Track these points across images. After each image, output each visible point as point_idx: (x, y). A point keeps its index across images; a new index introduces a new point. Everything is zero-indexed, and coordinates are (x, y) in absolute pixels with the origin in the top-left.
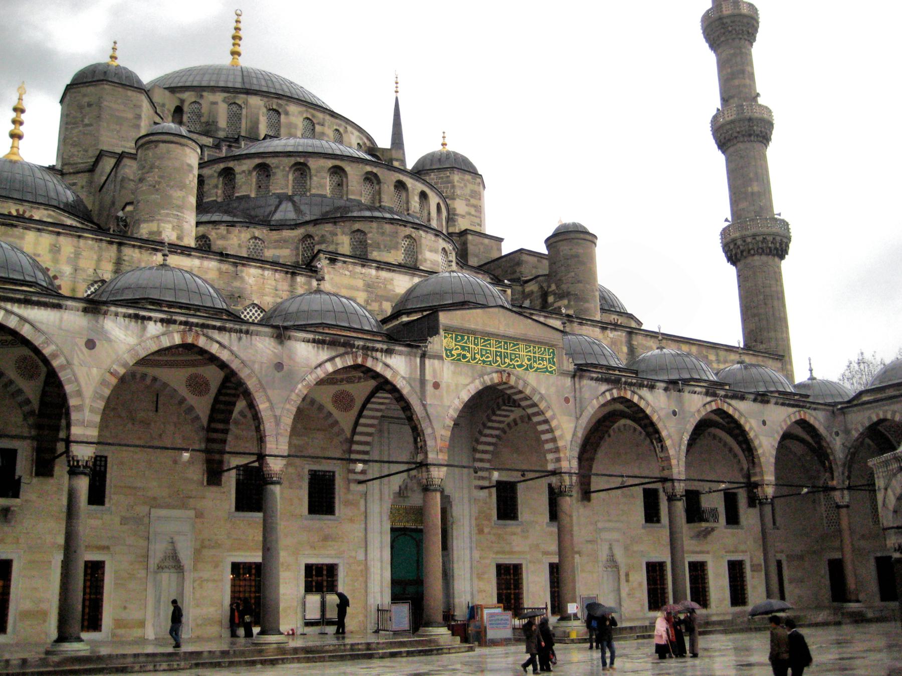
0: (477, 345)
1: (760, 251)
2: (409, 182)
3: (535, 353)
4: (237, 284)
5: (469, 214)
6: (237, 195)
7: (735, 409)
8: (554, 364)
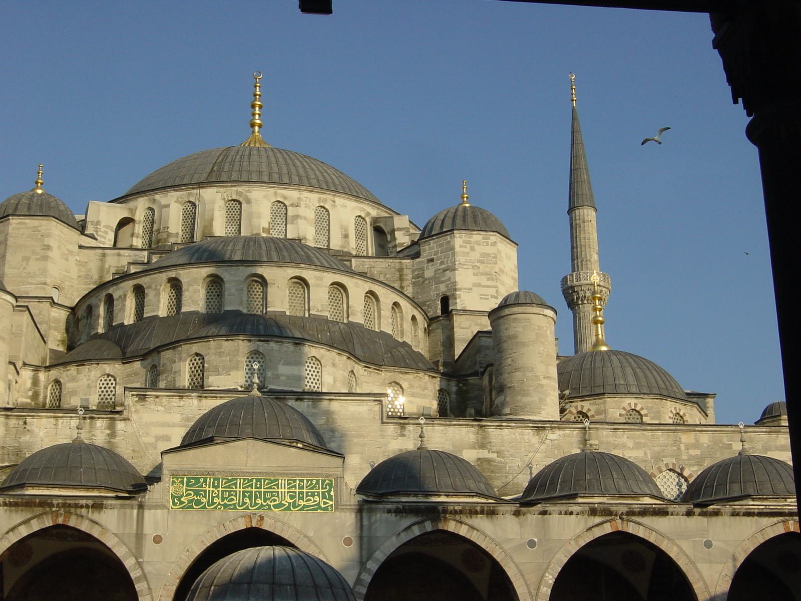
2: (308, 274)
4: (26, 438)
5: (479, 285)
6: (114, 324)
7: (652, 530)
8: (330, 498)
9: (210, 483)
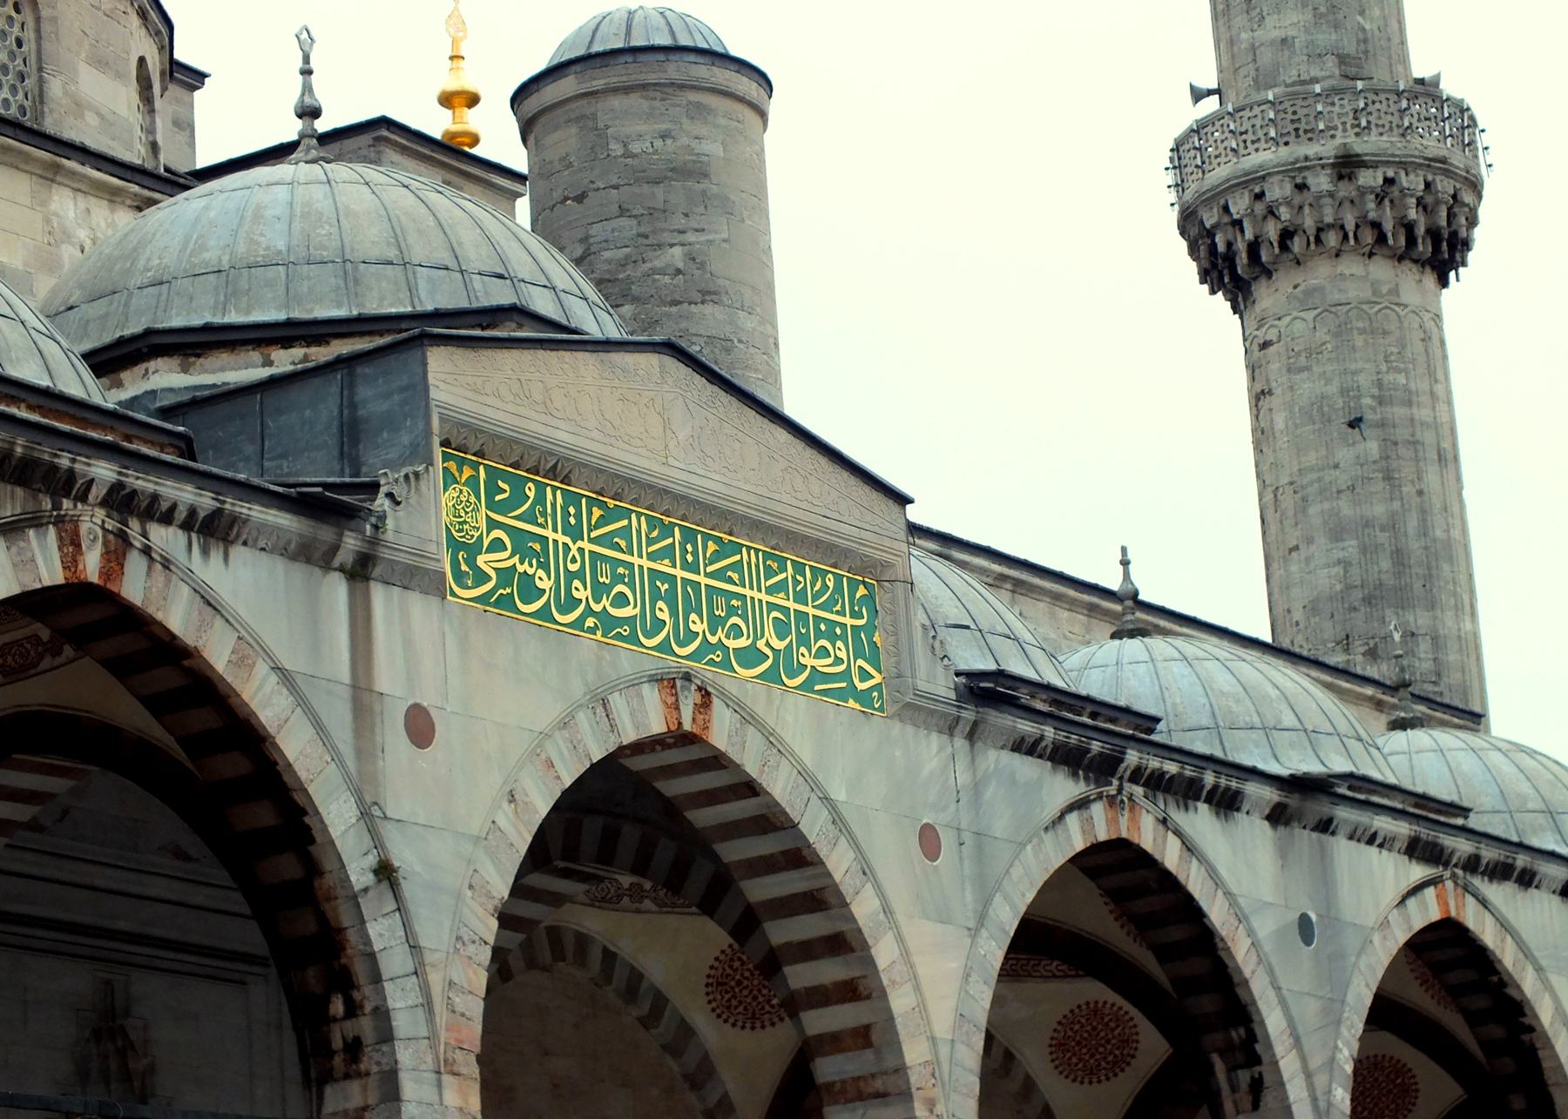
0: (576, 535)
1: (1368, 237)
3: (801, 597)
9: (554, 505)
